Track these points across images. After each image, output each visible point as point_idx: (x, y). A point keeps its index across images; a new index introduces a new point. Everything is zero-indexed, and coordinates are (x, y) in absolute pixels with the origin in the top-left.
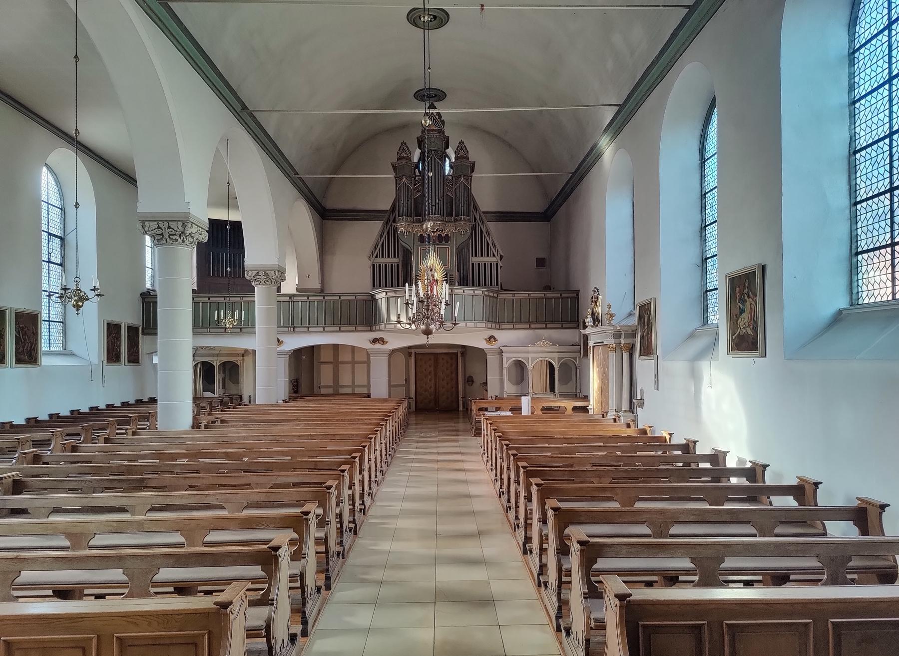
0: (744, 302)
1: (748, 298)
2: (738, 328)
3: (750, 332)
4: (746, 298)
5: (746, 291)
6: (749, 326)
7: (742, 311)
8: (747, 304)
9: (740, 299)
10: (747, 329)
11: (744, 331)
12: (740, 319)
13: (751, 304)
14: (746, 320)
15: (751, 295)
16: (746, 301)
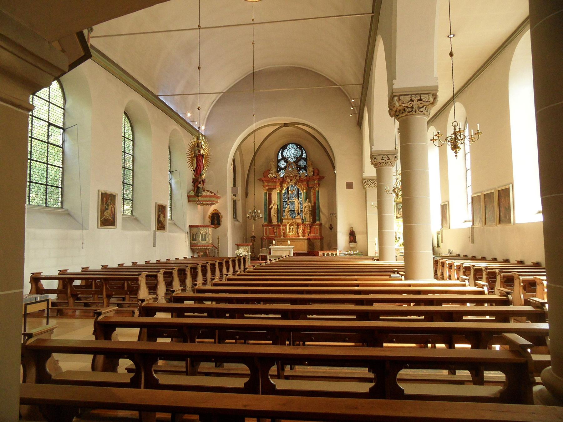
0: (108, 205)
1: (111, 204)
2: (104, 216)
3: (110, 219)
4: (109, 204)
5: (109, 201)
6: (110, 216)
7: (107, 209)
8: (110, 206)
9: (106, 203)
10: (109, 217)
11: (108, 218)
12: (105, 212)
13: (111, 207)
14: (109, 213)
15: (112, 204)
16: (109, 205)
